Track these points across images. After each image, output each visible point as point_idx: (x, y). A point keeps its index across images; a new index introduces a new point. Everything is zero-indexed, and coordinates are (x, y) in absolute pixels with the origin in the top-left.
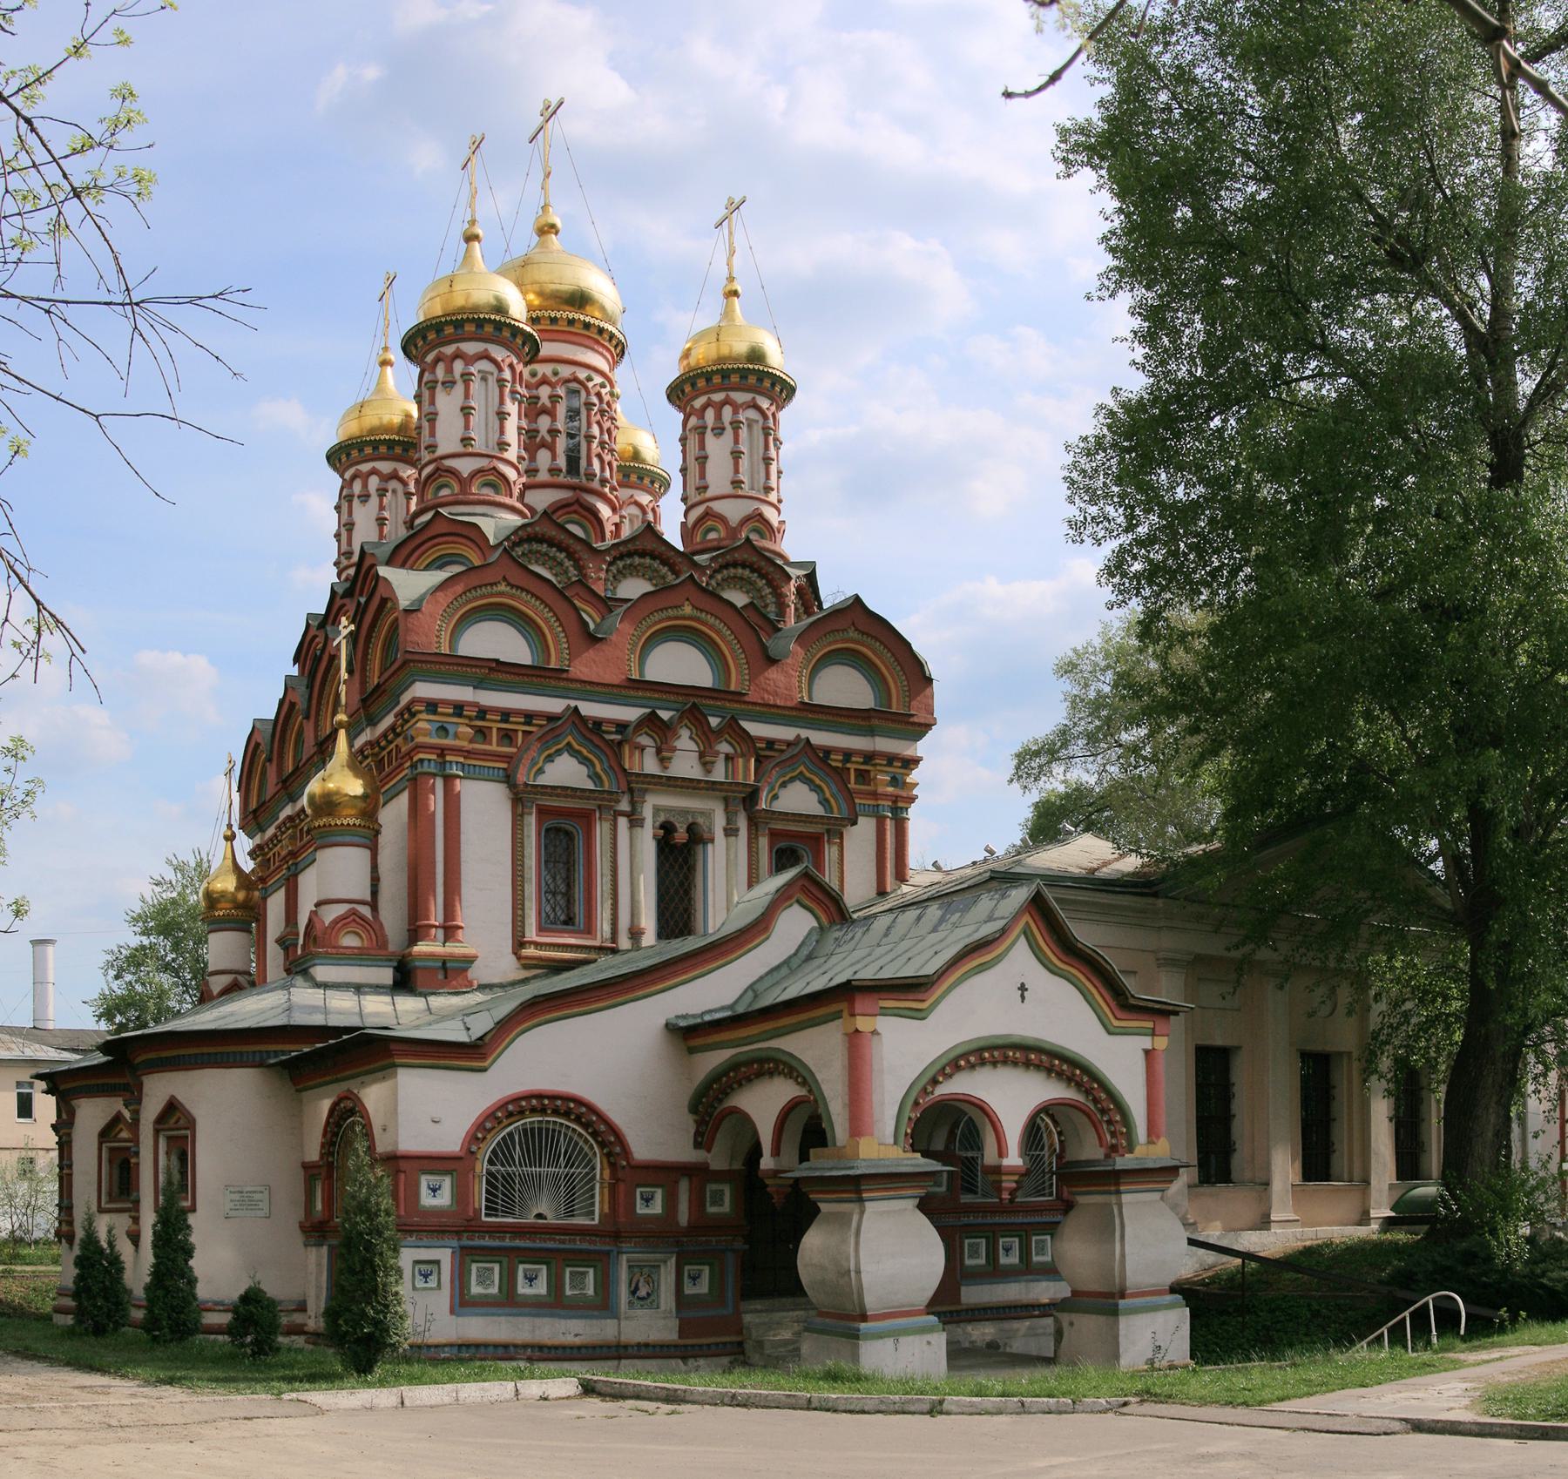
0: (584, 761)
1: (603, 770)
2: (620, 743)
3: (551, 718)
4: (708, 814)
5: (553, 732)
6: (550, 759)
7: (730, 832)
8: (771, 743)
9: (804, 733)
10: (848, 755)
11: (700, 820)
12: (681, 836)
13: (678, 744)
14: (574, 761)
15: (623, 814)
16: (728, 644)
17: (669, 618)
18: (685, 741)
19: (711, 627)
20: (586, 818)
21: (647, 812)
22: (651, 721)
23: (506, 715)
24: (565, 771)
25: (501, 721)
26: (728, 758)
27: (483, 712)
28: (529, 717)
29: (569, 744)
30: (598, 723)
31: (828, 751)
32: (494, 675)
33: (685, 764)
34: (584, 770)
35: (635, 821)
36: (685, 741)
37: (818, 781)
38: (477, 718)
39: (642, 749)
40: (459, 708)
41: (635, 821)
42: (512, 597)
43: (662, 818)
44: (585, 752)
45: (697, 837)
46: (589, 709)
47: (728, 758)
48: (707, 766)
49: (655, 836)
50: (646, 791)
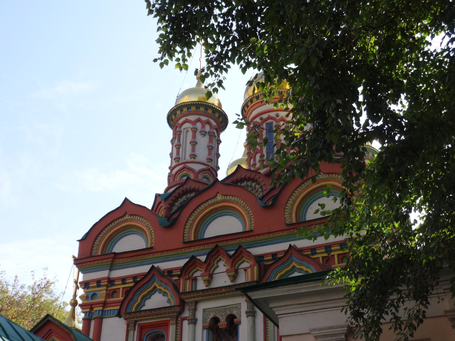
0: (165, 294)
1: (171, 296)
2: (179, 279)
3: (146, 275)
4: (238, 307)
5: (141, 282)
6: (145, 298)
7: (251, 314)
8: (274, 255)
9: (292, 243)
10: (328, 247)
11: (235, 312)
12: (223, 323)
13: (217, 271)
14: (161, 295)
15: (185, 319)
16: (243, 207)
17: (210, 205)
18: (222, 266)
19: (233, 202)
20: (166, 325)
21: (199, 315)
22: (193, 262)
23: (123, 280)
24: (157, 301)
25: (124, 283)
26: (245, 270)
27: (111, 281)
28: (134, 277)
29: (155, 287)
30: (170, 272)
31: (313, 250)
32: (117, 261)
33: (222, 279)
34: (166, 299)
35: (194, 321)
36: (222, 266)
37: (305, 269)
38: (112, 285)
39: (195, 279)
40: (98, 282)
41: (194, 321)
42: (131, 220)
43: (212, 316)
44: (162, 289)
45: (233, 323)
46: (164, 266)
47: (245, 270)
48: (234, 278)
49: (204, 328)
50: (196, 303)
